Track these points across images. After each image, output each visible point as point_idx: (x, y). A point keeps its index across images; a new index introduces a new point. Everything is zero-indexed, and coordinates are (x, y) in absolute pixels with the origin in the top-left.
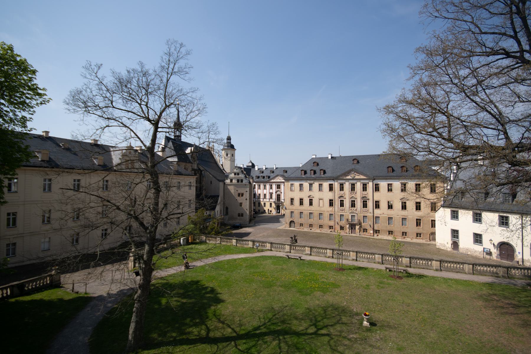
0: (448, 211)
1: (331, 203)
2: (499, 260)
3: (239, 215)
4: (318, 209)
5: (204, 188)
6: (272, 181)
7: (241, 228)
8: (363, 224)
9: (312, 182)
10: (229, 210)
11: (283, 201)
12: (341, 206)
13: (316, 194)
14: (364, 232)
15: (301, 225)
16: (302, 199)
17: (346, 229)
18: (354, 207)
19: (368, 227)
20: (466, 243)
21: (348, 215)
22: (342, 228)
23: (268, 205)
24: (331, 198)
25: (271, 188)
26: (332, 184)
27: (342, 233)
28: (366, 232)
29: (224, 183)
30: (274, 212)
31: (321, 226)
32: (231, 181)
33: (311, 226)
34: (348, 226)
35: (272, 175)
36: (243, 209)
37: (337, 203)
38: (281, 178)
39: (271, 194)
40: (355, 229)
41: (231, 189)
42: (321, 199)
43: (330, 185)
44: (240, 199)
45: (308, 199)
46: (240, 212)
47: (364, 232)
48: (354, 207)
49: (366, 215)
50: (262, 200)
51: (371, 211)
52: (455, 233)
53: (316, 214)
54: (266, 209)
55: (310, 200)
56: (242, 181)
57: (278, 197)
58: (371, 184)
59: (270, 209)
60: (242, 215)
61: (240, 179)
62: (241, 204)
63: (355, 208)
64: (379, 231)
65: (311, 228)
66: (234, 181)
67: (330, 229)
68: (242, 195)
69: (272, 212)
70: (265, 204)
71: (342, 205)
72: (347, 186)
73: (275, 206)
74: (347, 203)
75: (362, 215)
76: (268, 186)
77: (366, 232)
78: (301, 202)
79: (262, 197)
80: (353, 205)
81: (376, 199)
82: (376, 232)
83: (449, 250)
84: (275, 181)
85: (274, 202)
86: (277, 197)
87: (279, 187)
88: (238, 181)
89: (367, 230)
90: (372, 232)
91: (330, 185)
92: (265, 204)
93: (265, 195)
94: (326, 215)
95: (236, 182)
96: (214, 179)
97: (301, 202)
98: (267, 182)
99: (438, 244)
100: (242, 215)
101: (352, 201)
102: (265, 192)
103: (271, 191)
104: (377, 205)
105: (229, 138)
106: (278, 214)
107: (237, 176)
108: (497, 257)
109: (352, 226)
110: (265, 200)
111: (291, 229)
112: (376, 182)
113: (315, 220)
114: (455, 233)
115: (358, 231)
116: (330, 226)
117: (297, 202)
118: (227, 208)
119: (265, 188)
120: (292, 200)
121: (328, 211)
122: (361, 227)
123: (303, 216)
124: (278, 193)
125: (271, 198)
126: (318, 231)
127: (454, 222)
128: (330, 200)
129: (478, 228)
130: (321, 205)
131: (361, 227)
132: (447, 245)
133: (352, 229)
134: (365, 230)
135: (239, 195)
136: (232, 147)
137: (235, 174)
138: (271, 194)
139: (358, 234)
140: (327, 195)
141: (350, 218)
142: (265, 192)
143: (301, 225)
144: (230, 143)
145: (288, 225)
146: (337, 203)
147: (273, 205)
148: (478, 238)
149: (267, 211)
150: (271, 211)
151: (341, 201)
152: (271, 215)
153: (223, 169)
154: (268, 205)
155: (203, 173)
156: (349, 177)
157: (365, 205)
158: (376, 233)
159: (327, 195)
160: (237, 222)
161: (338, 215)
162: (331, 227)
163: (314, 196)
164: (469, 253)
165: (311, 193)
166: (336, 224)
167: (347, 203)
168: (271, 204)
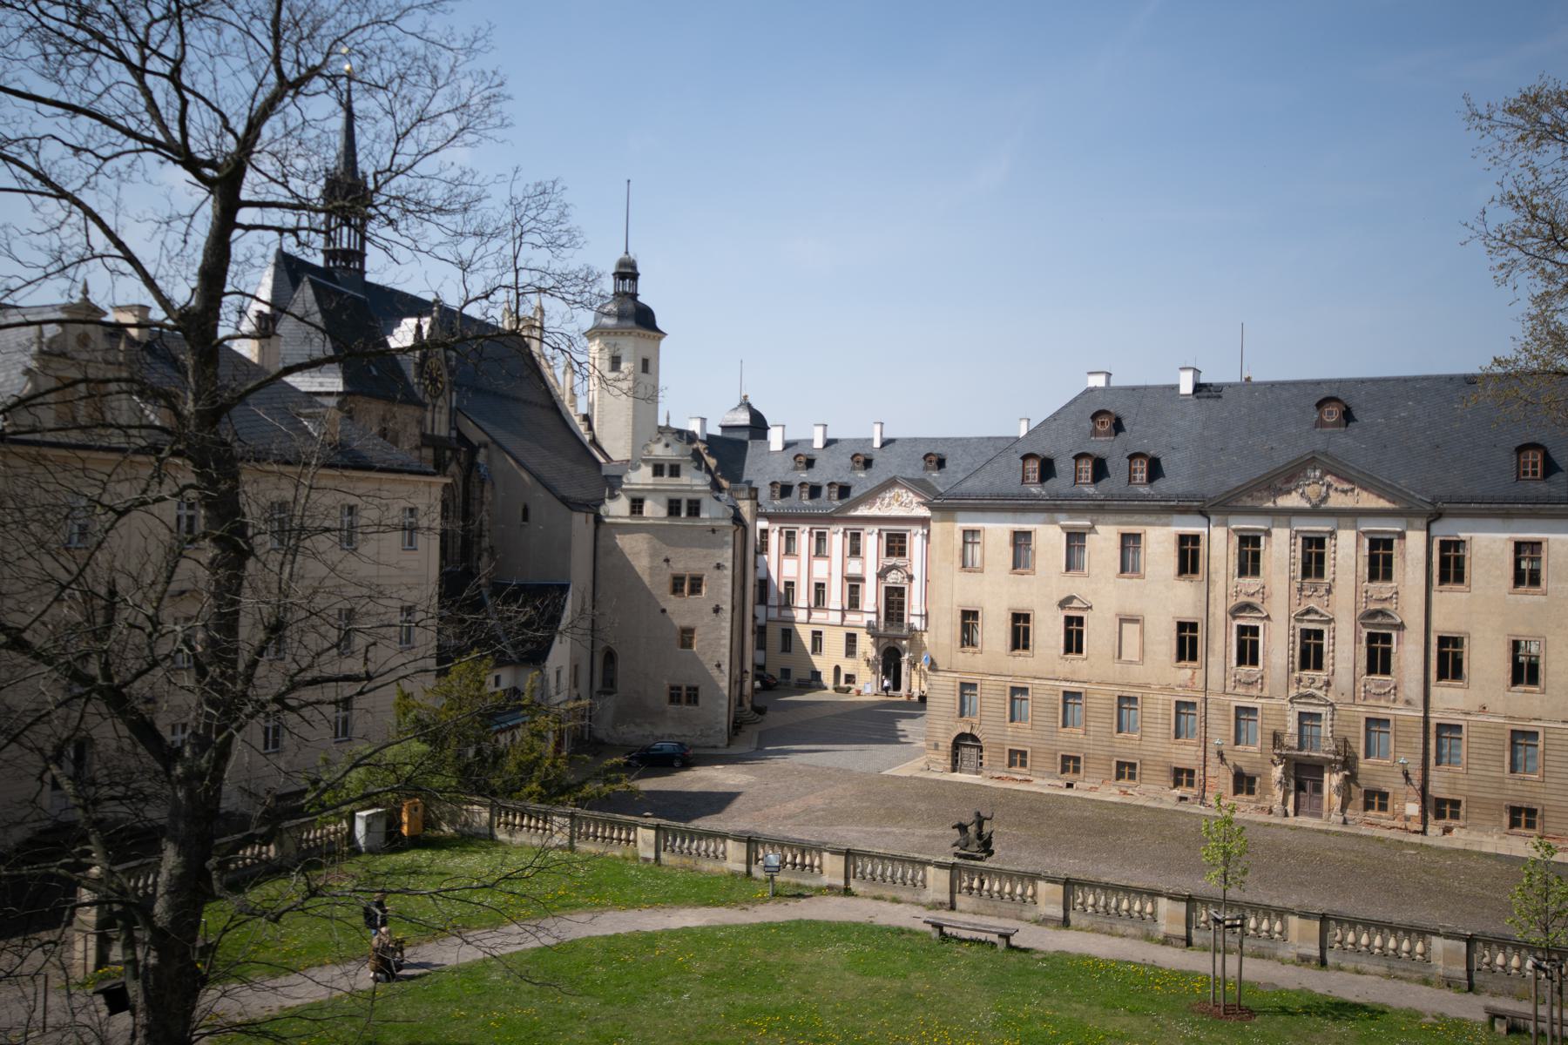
1: (1187, 642)
3: (675, 696)
4: (1114, 671)
5: (486, 543)
6: (862, 511)
7: (687, 763)
8: (1363, 765)
9: (1082, 522)
10: (621, 667)
11: (917, 623)
12: (1241, 661)
13: (1102, 588)
14: (1368, 806)
15: (1017, 757)
16: (1026, 617)
17: (1267, 790)
18: (1319, 666)
19: (1392, 783)
21: (1282, 713)
22: (1244, 782)
23: (834, 642)
24: (1188, 615)
25: (855, 551)
26: (1195, 539)
27: (1246, 810)
28: (1383, 807)
29: (598, 520)
30: (868, 685)
31: (1125, 770)
32: (637, 505)
33: (1070, 763)
34: (1277, 772)
35: (861, 480)
36: (696, 661)
37: (1220, 643)
38: (908, 496)
39: (854, 585)
40: (1318, 788)
41: (637, 550)
43: (1183, 539)
44: (681, 610)
45: (1061, 616)
46: (684, 679)
47: (1368, 806)
48: (1319, 666)
49: (1382, 713)
50: (801, 615)
51: (1413, 689)
53: (1100, 701)
54: (824, 664)
55: (1069, 620)
56: (694, 508)
57: (894, 601)
58: (1415, 541)
59: (847, 667)
60: (693, 696)
61: (684, 498)
63: (1322, 676)
64: (1456, 804)
65: (1069, 777)
66: (654, 510)
67: (1177, 783)
68: (696, 585)
69: (859, 685)
70: (817, 636)
71: (1248, 652)
72: (1280, 549)
73: (872, 653)
74: (1277, 646)
75: (1362, 712)
76: (837, 540)
77: (1383, 807)
78: (1020, 631)
79: (802, 598)
80: (1311, 653)
81: (1441, 625)
82: (1440, 808)
85: (871, 629)
86: (889, 604)
87: (896, 545)
88: (674, 508)
89: (1384, 796)
90: (1413, 809)
91: (1183, 539)
92: (817, 636)
93: (820, 587)
94: (1158, 709)
95: (663, 512)
96: (542, 494)
97: (1020, 631)
98: (831, 519)
100: (693, 696)
101: (1306, 634)
102: (820, 570)
103: (854, 567)
104: (1449, 660)
105: (627, 272)
107: (666, 479)
109: (1304, 776)
110: (817, 616)
111: (959, 777)
112: (1447, 529)
113: (1093, 735)
115: (1337, 800)
116: (1178, 772)
117: (994, 631)
118: (610, 657)
119: (820, 551)
120: (969, 618)
121: (1167, 688)
122: (1351, 779)
123: (1027, 707)
124: (894, 578)
125: (854, 604)
126: (1111, 793)
128: (1182, 626)
130: (1131, 650)
131: (1351, 779)
133: (1300, 787)
134: (1376, 799)
135: (677, 585)
136: (644, 319)
137: (658, 470)
138: (854, 585)
139: (1336, 817)
140: (1166, 596)
141: (1292, 726)
142: (820, 570)
143: (1017, 757)
144: (634, 296)
145: (943, 758)
147: (865, 644)
149: (827, 678)
150: (850, 678)
151: (1242, 630)
152: (852, 697)
153: (594, 441)
154: (834, 642)
155: (481, 457)
156: (1292, 501)
157: (1379, 658)
158: (1440, 815)
159: (1166, 596)
160: (666, 732)
161: (1223, 709)
162: (1181, 776)
163: (1090, 599)
165: (1074, 585)
166: (1213, 759)
167: (1277, 646)
168: (851, 639)
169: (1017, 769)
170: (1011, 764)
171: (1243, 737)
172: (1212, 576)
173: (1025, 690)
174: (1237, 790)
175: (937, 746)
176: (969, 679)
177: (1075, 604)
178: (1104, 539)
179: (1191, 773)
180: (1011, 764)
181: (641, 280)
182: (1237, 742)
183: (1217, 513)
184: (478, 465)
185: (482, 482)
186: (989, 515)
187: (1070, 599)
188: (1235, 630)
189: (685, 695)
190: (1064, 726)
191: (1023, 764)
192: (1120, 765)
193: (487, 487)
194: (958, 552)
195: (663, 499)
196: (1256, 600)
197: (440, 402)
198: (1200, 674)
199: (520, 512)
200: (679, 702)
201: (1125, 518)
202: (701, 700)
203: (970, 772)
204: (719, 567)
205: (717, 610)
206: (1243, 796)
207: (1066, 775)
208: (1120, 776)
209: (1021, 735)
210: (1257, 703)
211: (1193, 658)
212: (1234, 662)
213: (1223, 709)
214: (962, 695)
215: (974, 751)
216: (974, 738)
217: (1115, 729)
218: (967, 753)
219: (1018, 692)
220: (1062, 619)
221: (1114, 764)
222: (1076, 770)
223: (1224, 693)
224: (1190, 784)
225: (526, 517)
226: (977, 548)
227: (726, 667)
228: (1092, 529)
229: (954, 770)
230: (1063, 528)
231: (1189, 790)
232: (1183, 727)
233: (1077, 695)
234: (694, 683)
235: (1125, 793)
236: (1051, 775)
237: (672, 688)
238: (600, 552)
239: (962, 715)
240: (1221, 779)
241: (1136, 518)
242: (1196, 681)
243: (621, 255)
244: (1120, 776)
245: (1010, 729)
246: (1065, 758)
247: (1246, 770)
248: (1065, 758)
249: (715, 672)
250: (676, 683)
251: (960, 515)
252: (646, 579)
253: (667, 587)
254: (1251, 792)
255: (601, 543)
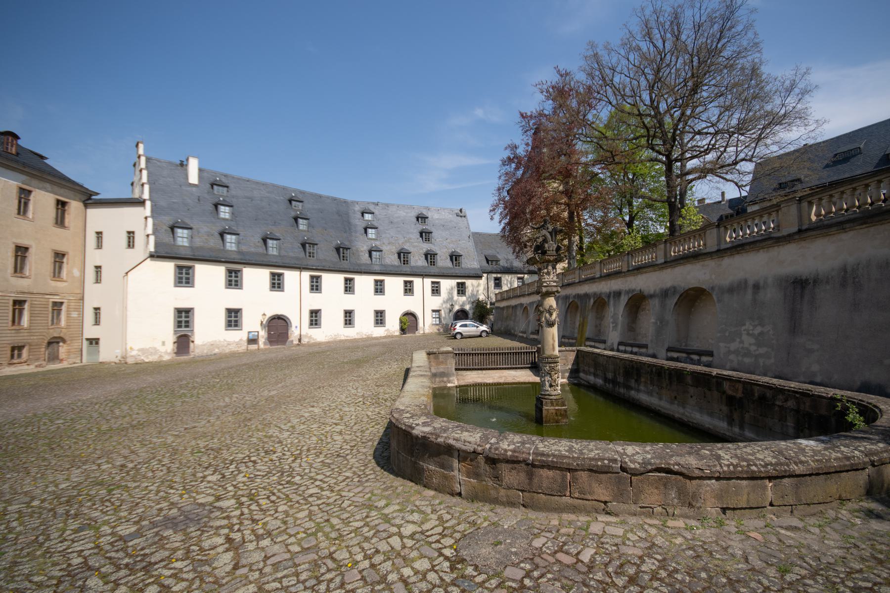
0: (168, 268)
2: (268, 346)
20: (209, 333)
52: (184, 317)
83: (166, 358)
99: (134, 353)
108: (265, 344)
114: (184, 317)
127: (184, 291)
129: (234, 298)
132: (162, 349)
148: (233, 318)
164: (217, 351)
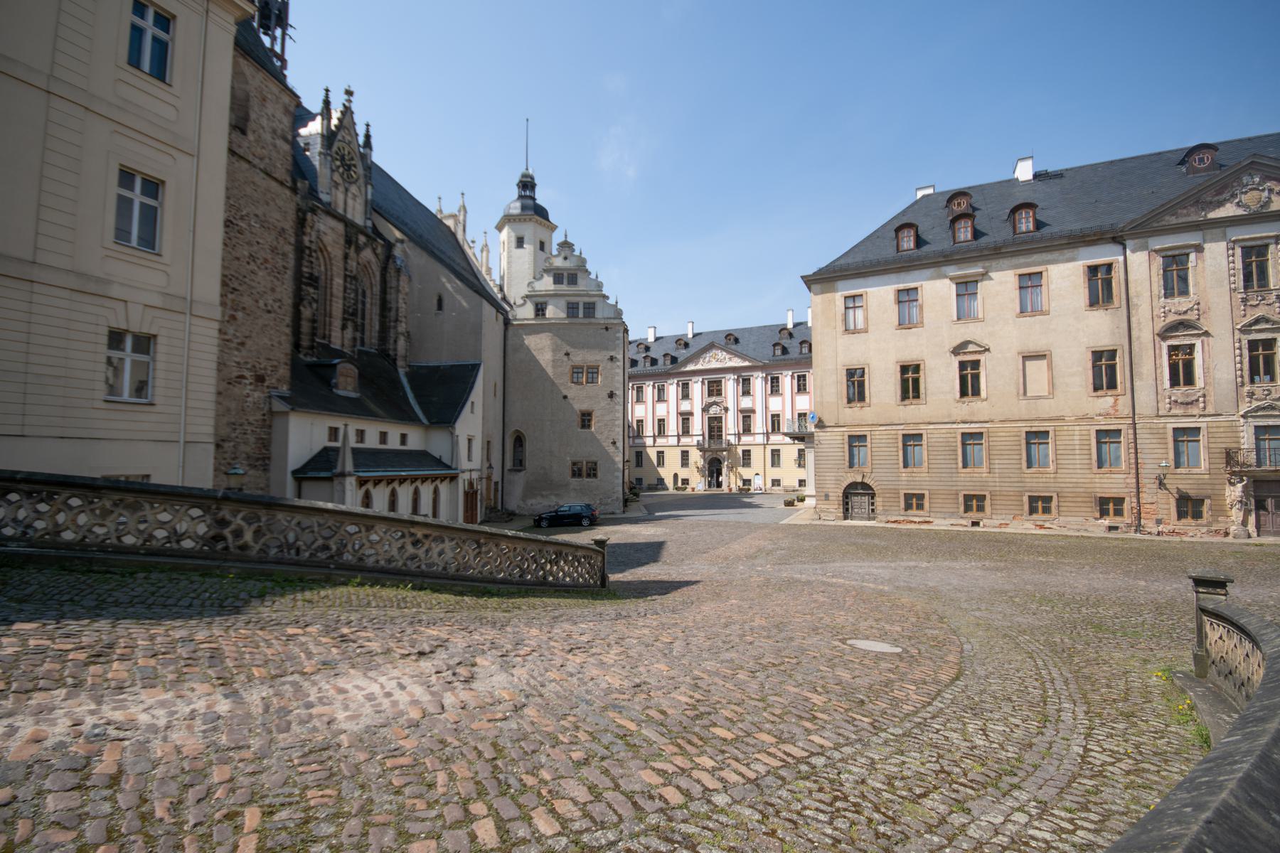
1: (1104, 370)
4: (1021, 408)
5: (402, 328)
6: (690, 367)
7: (594, 522)
9: (976, 269)
10: (528, 446)
11: (732, 439)
12: (1174, 382)
15: (914, 501)
16: (917, 368)
22: (1189, 506)
23: (673, 458)
24: (1104, 343)
25: (686, 396)
27: (1194, 532)
30: (698, 484)
31: (1039, 504)
33: (974, 502)
35: (682, 354)
36: (594, 439)
38: (722, 355)
39: (685, 417)
41: (541, 347)
42: (1040, 356)
43: (1093, 270)
45: (955, 362)
46: (584, 454)
50: (649, 441)
53: (1006, 439)
54: (666, 473)
57: (715, 427)
59: (683, 473)
60: (592, 471)
61: (581, 300)
62: (586, 419)
65: (974, 515)
67: (1104, 513)
69: (692, 484)
70: (660, 454)
71: (1182, 372)
73: (701, 463)
76: (672, 389)
78: (910, 381)
79: (649, 430)
84: (699, 366)
85: (700, 447)
86: (711, 429)
87: (714, 389)
88: (572, 309)
91: (1093, 270)
92: (660, 454)
93: (661, 423)
97: (910, 381)
98: (668, 375)
102: (661, 410)
103: (685, 406)
105: (527, 185)
106: (715, 491)
107: (564, 288)
110: (660, 441)
111: (849, 522)
117: (884, 386)
118: (519, 441)
119: (661, 398)
121: (1085, 418)
123: (922, 452)
124: (714, 410)
125: (686, 431)
126: (1025, 526)
128: (1097, 355)
137: (558, 279)
138: (685, 417)
142: (661, 410)
143: (914, 501)
144: (534, 199)
145: (835, 508)
146: (1145, 367)
147: (696, 457)
149: (669, 482)
150: (686, 481)
151: (1173, 349)
152: (689, 491)
153: (504, 298)
154: (673, 458)
155: (397, 252)
160: (571, 503)
162: (1107, 505)
163: (986, 342)
168: (685, 455)
169: (914, 512)
170: (908, 507)
171: (1184, 459)
172: (1134, 300)
173: (919, 436)
174: (1181, 515)
175: (827, 497)
176: (857, 431)
177: (971, 348)
178: (1001, 284)
179: (1119, 501)
180: (908, 507)
181: (537, 190)
182: (1177, 466)
183: (1134, 236)
184: (395, 257)
185: (398, 271)
186: (871, 280)
187: (965, 344)
188: (1165, 351)
189: (586, 470)
190: (965, 466)
191: (920, 507)
192: (1033, 500)
193: (403, 278)
194: (840, 318)
195: (562, 303)
196: (1192, 316)
197: (353, 189)
198: (1124, 402)
199: (435, 301)
200: (580, 475)
201: (1022, 260)
202: (599, 474)
203: (862, 519)
204: (612, 359)
205: (611, 395)
206: (1189, 521)
207: (969, 514)
208: (1033, 510)
209: (917, 479)
210: (1202, 423)
211: (1112, 385)
212: (1167, 384)
213: (1159, 434)
214: (851, 447)
215: (866, 499)
216: (864, 486)
217: (1024, 464)
218: (860, 502)
219: (912, 439)
220: (957, 365)
221: (1026, 499)
222: (981, 509)
223: (1158, 416)
224: (1119, 513)
225: (440, 306)
226: (859, 313)
227: (620, 444)
228: (984, 276)
229: (846, 518)
230: (951, 279)
231: (1118, 519)
232: (1106, 456)
233: (979, 435)
234: (594, 459)
235: (1041, 527)
236: (952, 515)
237: (574, 464)
238: (509, 348)
239: (851, 465)
240: (1162, 505)
241: (1036, 257)
242: (1120, 407)
243: (523, 170)
244: (1033, 510)
245: (904, 475)
246: (968, 498)
247: (1192, 493)
248: (968, 498)
249: (611, 449)
250: (577, 459)
251: (840, 284)
252: (550, 371)
253: (567, 378)
254: (1197, 515)
255: (510, 342)
